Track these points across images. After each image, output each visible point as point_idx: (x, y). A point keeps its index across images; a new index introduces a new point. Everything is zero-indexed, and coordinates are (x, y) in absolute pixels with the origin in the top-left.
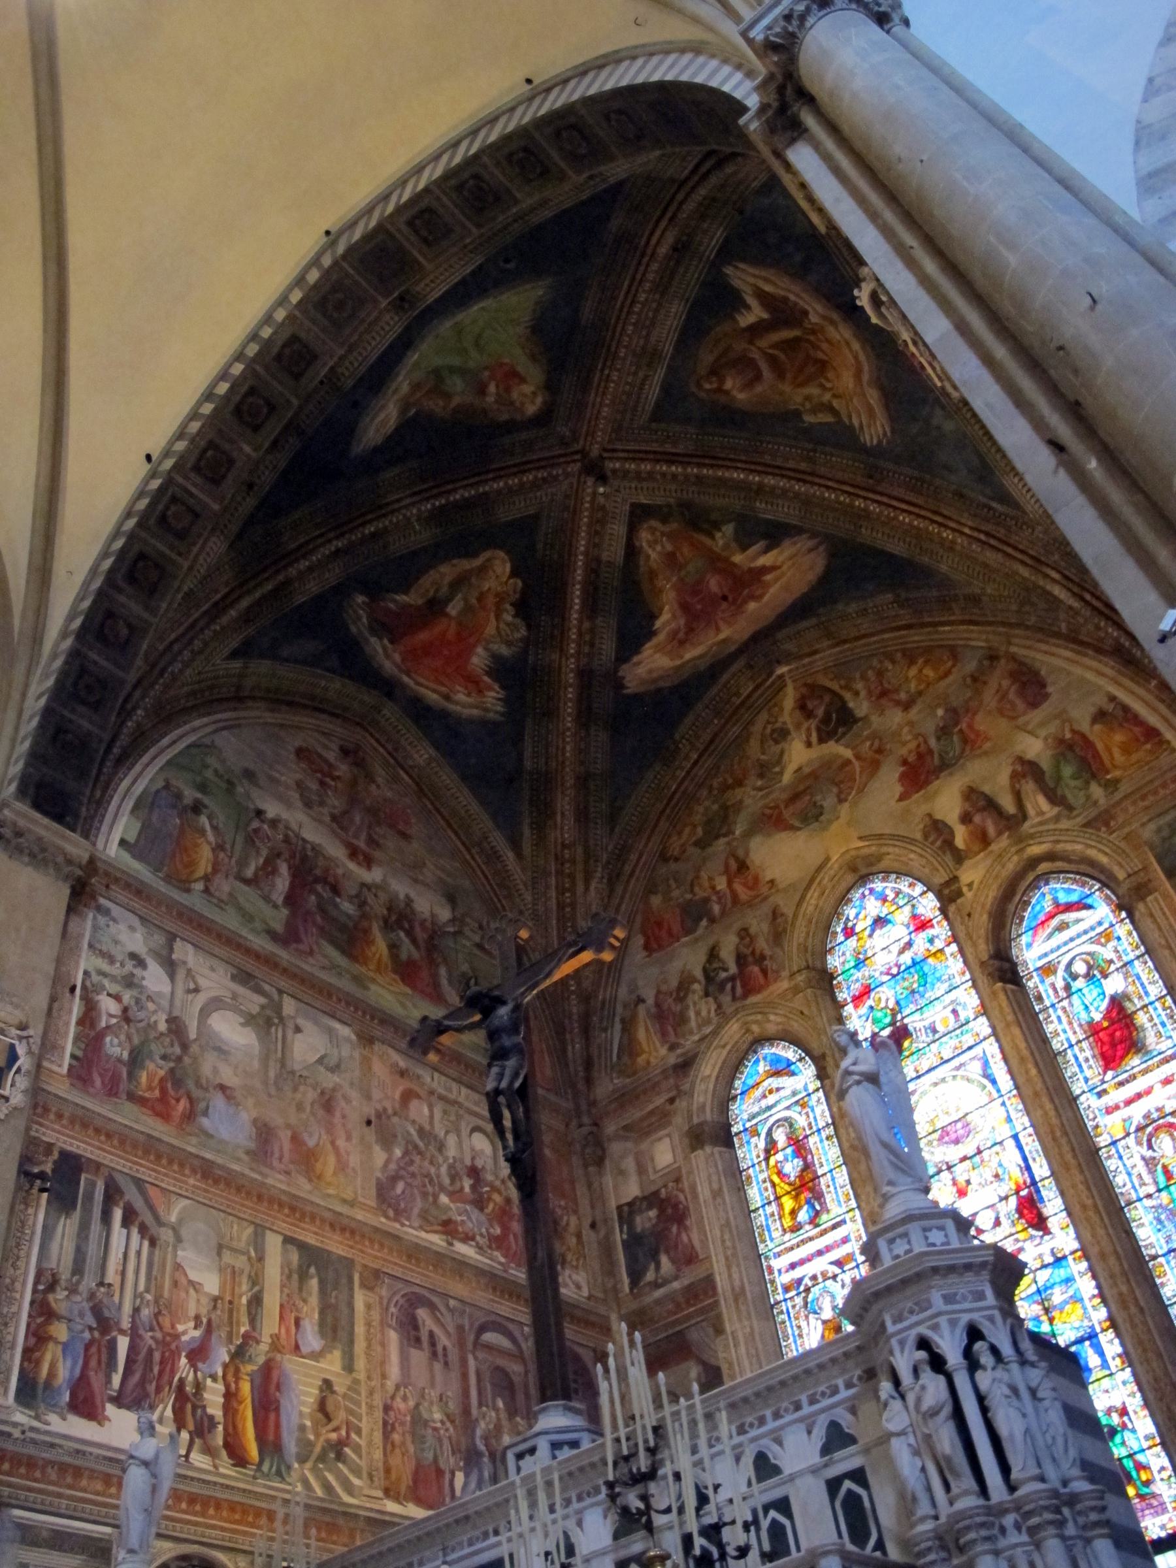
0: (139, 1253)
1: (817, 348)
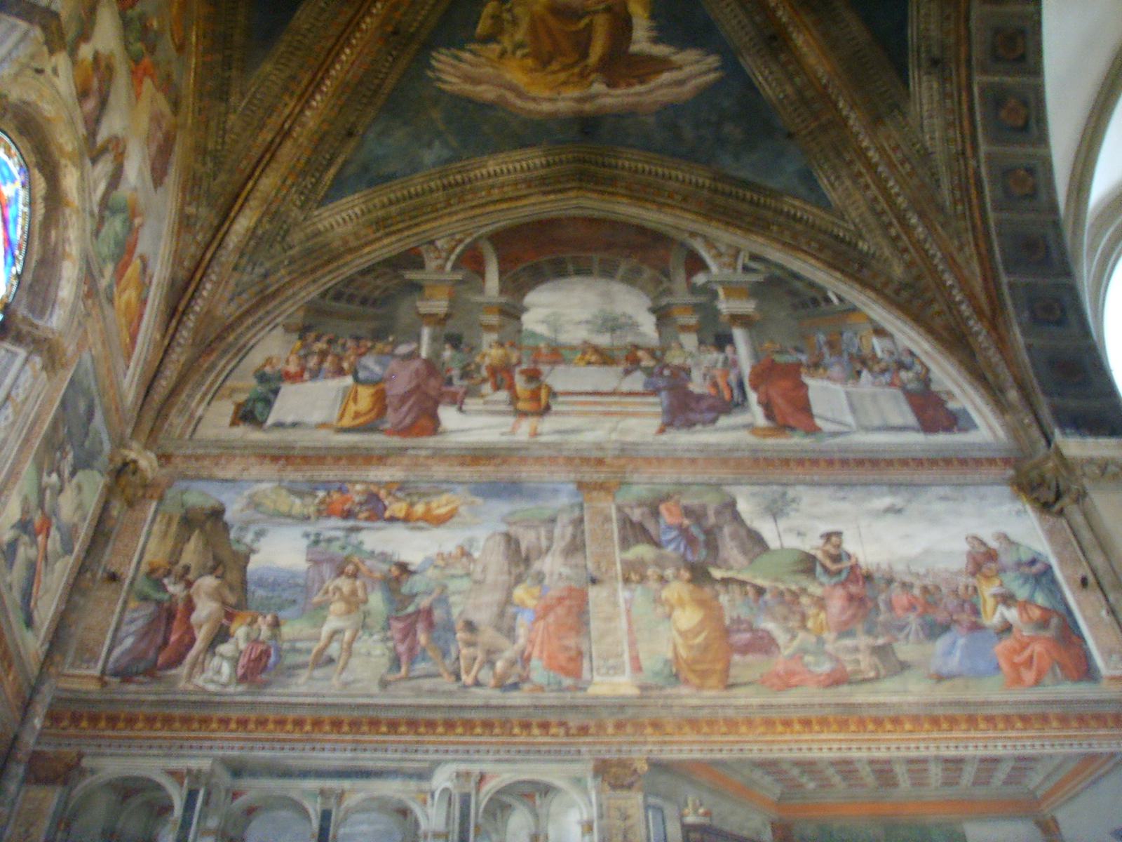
1: (563, 69)
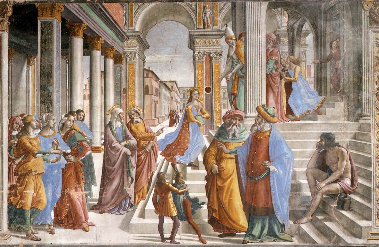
0: (104, 73)
